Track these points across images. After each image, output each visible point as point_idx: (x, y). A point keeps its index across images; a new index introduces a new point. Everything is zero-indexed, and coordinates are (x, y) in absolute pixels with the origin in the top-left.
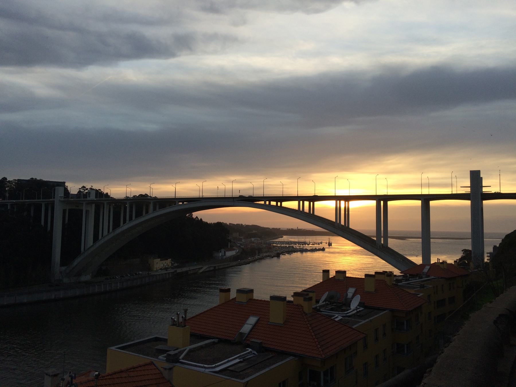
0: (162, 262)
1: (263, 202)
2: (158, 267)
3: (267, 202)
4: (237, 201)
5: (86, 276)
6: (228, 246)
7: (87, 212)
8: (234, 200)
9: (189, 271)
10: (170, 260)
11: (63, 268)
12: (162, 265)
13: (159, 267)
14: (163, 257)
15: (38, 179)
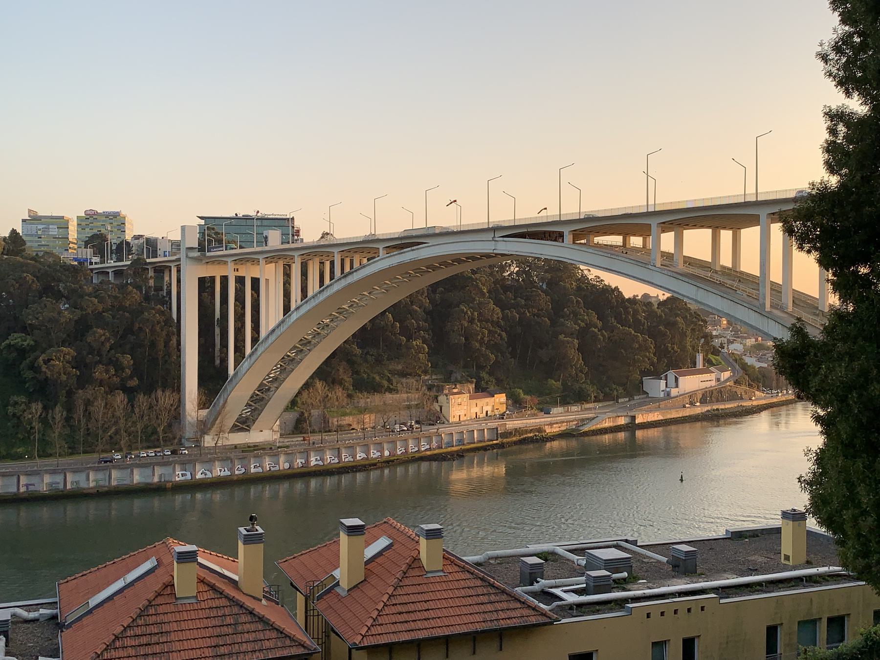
0: (475, 401)
1: (616, 240)
2: (462, 414)
3: (664, 236)
4: (501, 239)
5: (262, 431)
6: (694, 364)
7: (240, 280)
8: (494, 237)
9: (546, 427)
10: (501, 398)
11: (204, 413)
12: (477, 410)
13: (465, 415)
14: (482, 390)
15: (240, 215)
